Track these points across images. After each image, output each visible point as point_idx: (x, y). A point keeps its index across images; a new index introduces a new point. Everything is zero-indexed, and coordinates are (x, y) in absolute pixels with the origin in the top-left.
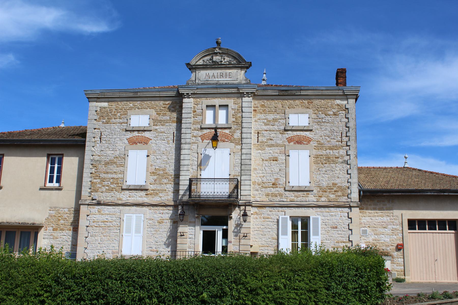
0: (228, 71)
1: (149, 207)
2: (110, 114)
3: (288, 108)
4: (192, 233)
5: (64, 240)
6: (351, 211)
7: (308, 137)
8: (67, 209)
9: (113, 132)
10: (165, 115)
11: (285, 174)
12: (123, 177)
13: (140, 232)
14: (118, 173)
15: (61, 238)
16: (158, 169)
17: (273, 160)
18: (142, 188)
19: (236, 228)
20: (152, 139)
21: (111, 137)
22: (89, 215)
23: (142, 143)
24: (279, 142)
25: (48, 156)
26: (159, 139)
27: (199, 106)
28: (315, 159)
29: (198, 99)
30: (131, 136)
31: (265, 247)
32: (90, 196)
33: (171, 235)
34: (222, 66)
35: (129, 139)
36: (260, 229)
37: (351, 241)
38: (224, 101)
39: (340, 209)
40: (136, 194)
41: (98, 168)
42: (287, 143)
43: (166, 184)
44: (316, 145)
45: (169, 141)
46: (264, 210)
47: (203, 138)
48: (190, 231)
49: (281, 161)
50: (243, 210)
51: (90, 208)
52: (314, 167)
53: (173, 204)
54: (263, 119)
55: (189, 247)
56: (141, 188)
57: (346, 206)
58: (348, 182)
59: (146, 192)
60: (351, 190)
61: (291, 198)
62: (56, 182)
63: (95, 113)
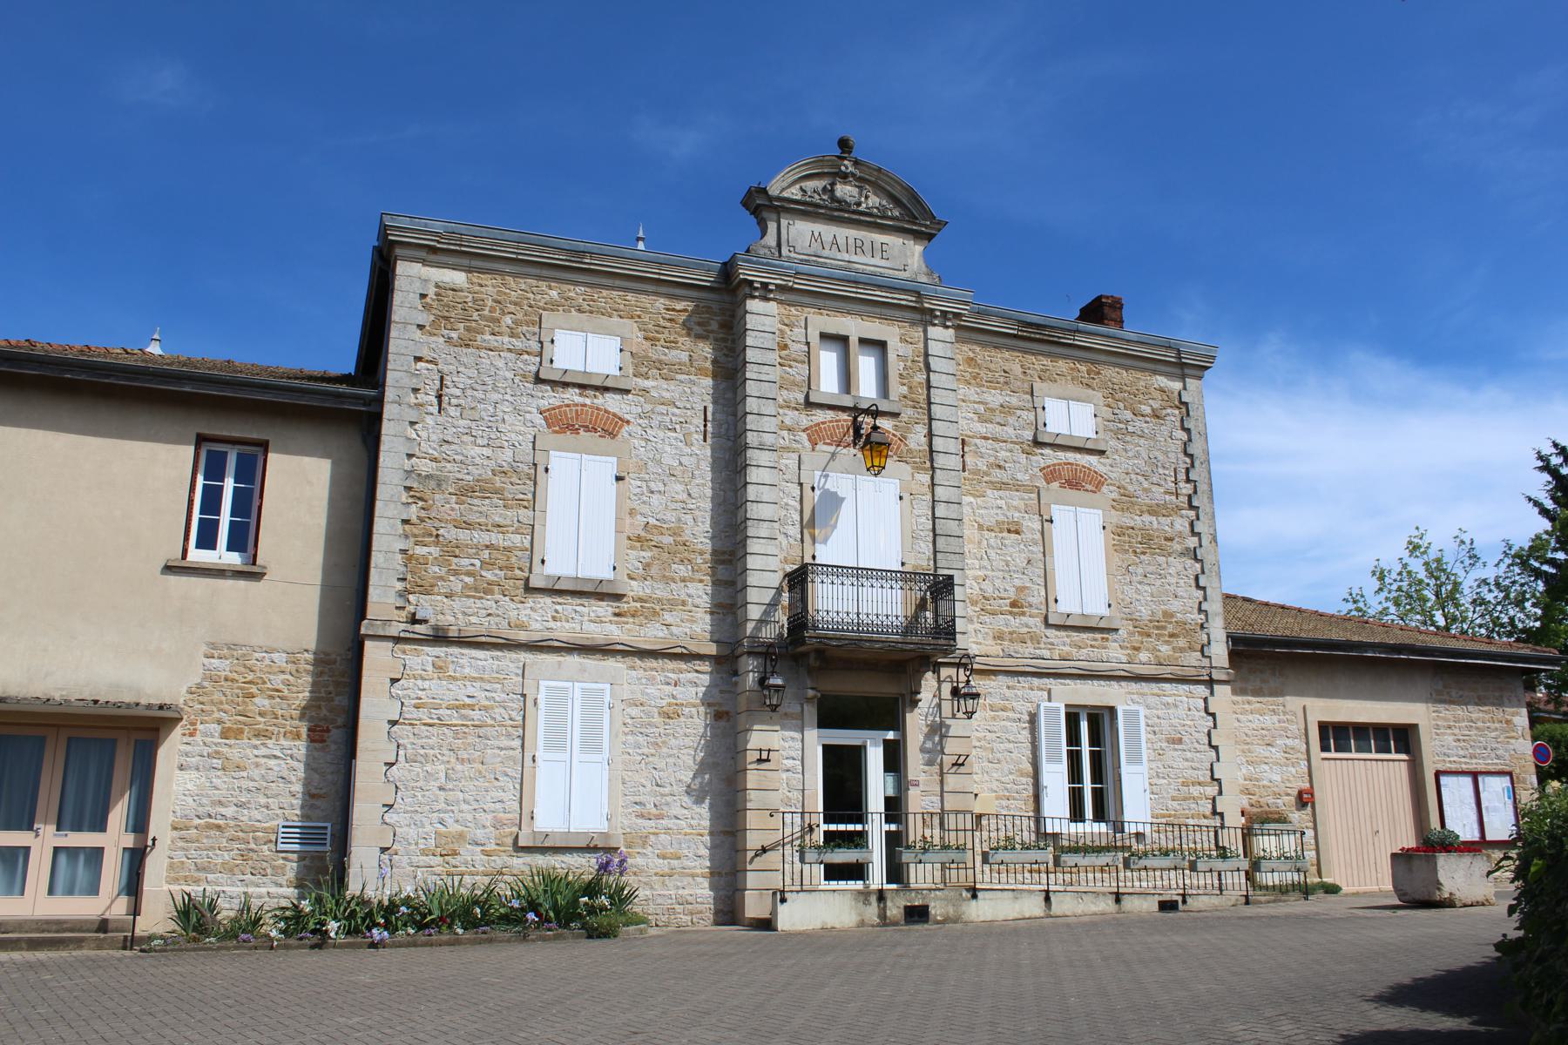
0: (879, 238)
1: (629, 660)
2: (477, 313)
3: (1038, 379)
4: (793, 754)
5: (272, 776)
6: (1212, 693)
7: (1096, 472)
8: (284, 655)
9: (489, 381)
10: (671, 344)
12: (528, 546)
13: (598, 749)
14: (511, 529)
15: (257, 765)
16: (655, 526)
17: (1009, 531)
19: (928, 736)
20: (632, 420)
21: (480, 395)
22: (398, 680)
23: (596, 431)
24: (1023, 477)
25: (201, 440)
26: (655, 423)
27: (795, 330)
28: (1117, 537)
29: (792, 309)
30: (558, 404)
32: (403, 608)
34: (862, 218)
35: (548, 410)
36: (983, 743)
37: (1217, 780)
38: (874, 328)
39: (1186, 687)
40: (578, 608)
41: (431, 506)
42: (1041, 483)
43: (683, 580)
44: (1115, 495)
45: (690, 434)
47: (815, 435)
48: (786, 745)
49: (1030, 536)
51: (404, 652)
52: (1117, 559)
53: (715, 653)
54: (975, 402)
57: (1202, 678)
58: (1200, 610)
59: (615, 604)
60: (1208, 635)
62: (230, 549)
63: (418, 303)
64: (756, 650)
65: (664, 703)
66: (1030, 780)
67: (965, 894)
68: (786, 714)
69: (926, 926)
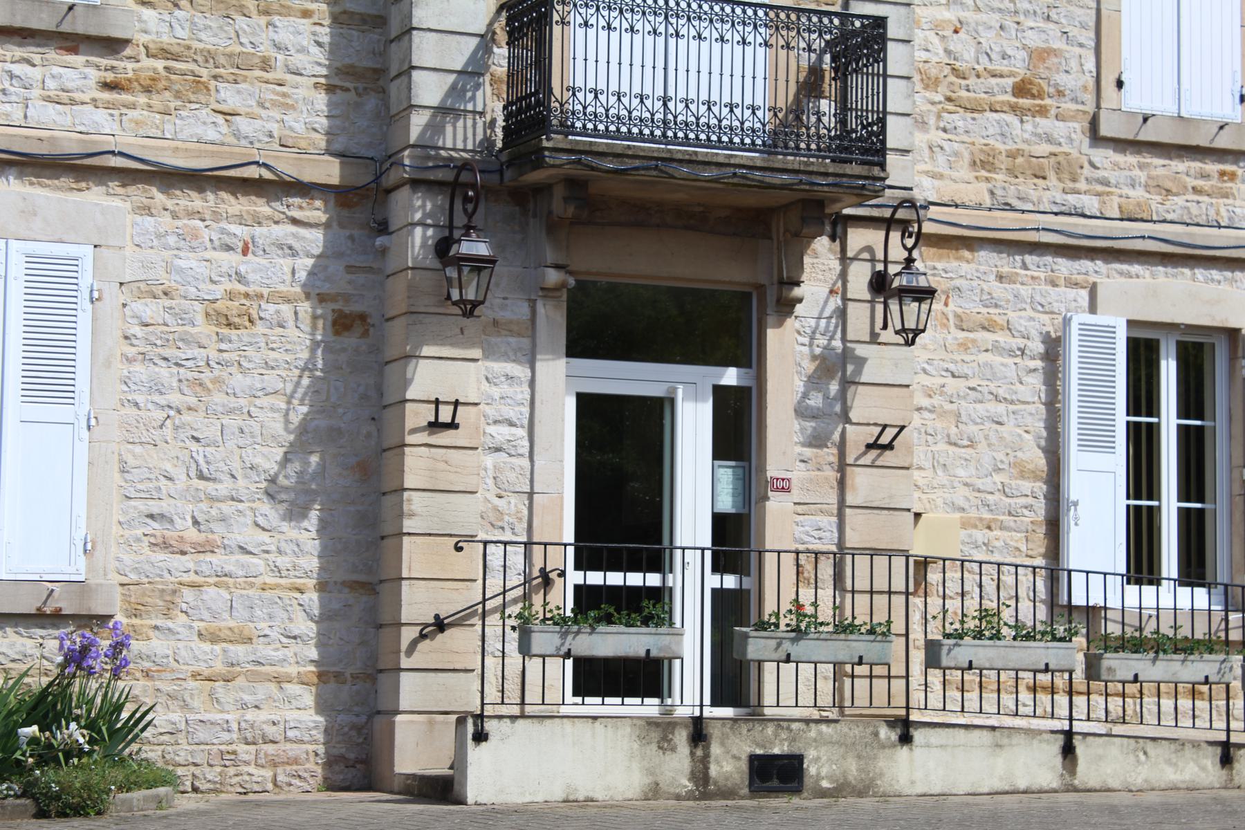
1: (138, 193)
4: (510, 413)
11: (1092, 24)
13: (66, 394)
18: (80, 29)
19: (816, 381)
31: (975, 527)
33: (322, 423)
36: (937, 400)
40: (18, 69)
43: (267, 13)
46: (965, 268)
48: (495, 392)
50: (866, 255)
53: (335, 180)
55: (492, 516)
56: (65, 28)
61: (1131, 193)
64: (431, 176)
65: (218, 291)
66: (1041, 488)
67: (884, 732)
68: (495, 323)
69: (796, 800)
